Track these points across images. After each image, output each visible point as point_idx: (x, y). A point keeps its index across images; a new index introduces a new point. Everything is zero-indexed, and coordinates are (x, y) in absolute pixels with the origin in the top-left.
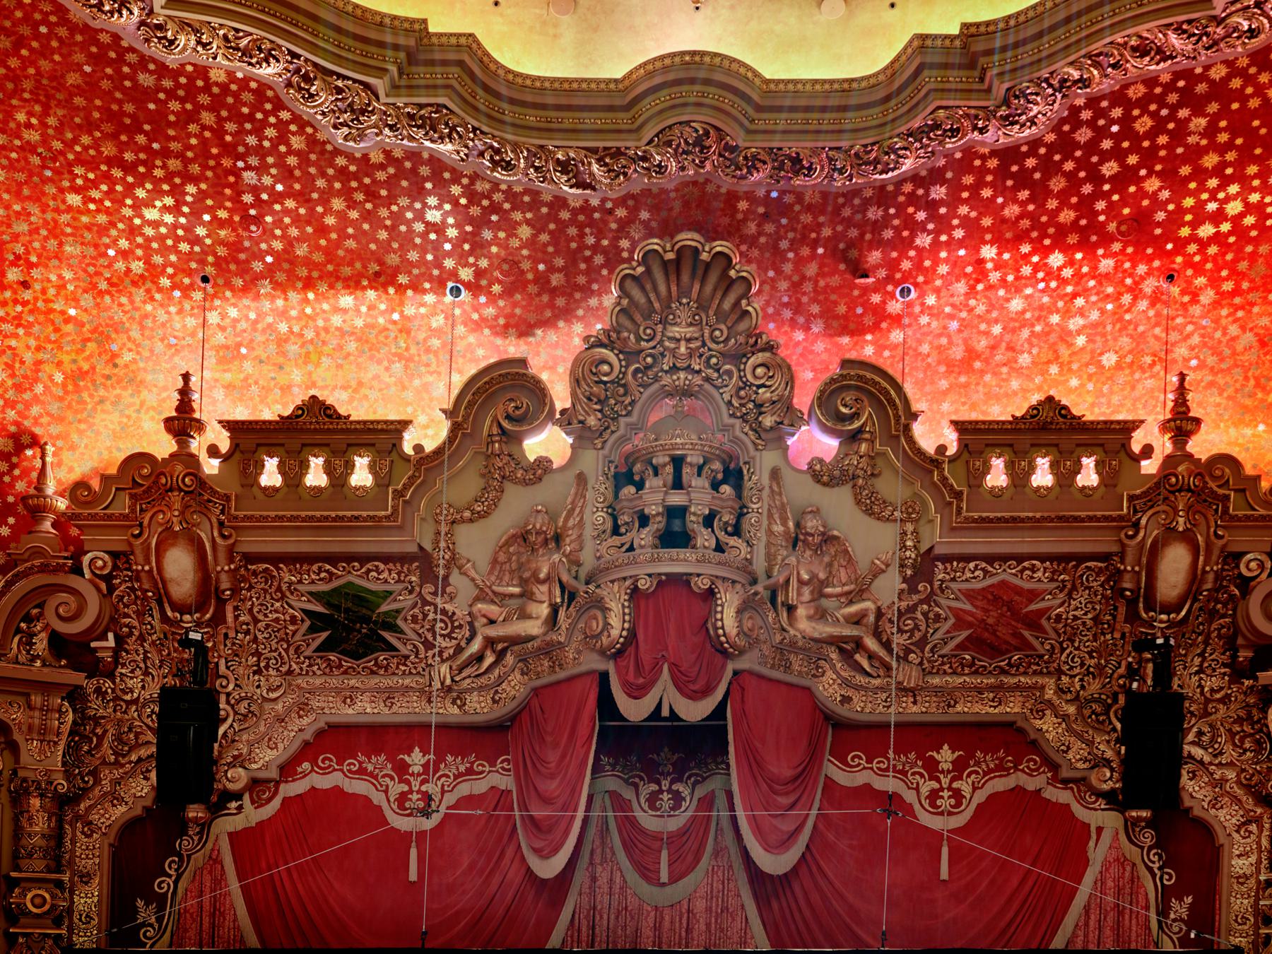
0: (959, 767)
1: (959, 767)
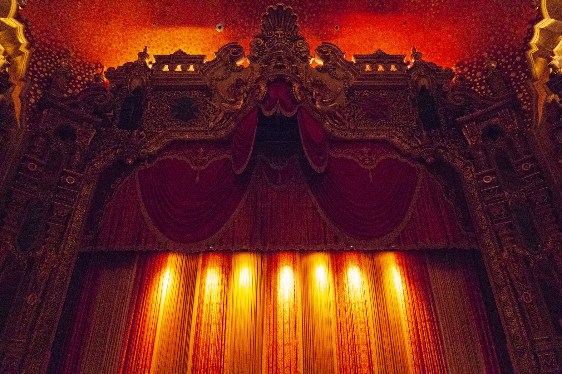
0: (370, 153)
1: (370, 153)
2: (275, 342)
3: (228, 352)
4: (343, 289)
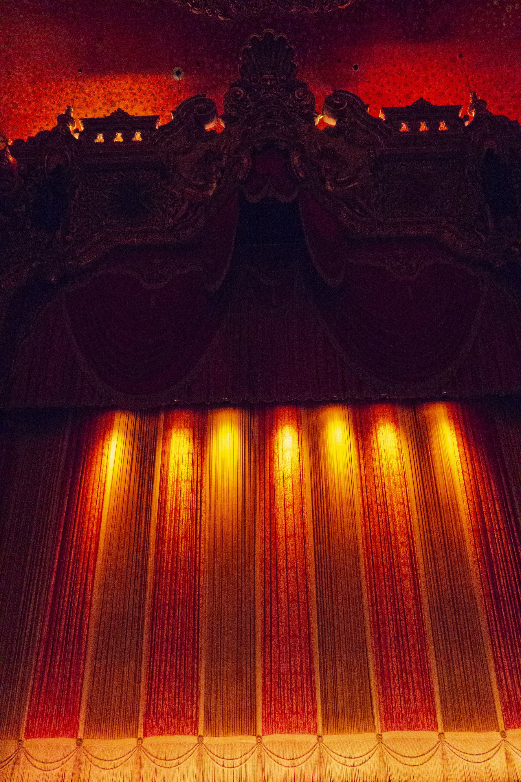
2: (273, 533)
3: (204, 547)
4: (371, 456)
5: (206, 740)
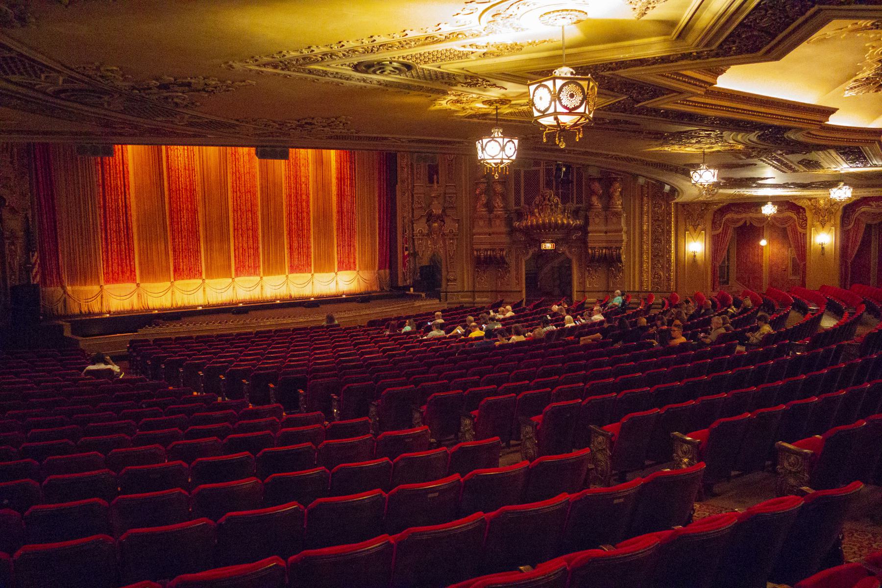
5: (207, 281)
